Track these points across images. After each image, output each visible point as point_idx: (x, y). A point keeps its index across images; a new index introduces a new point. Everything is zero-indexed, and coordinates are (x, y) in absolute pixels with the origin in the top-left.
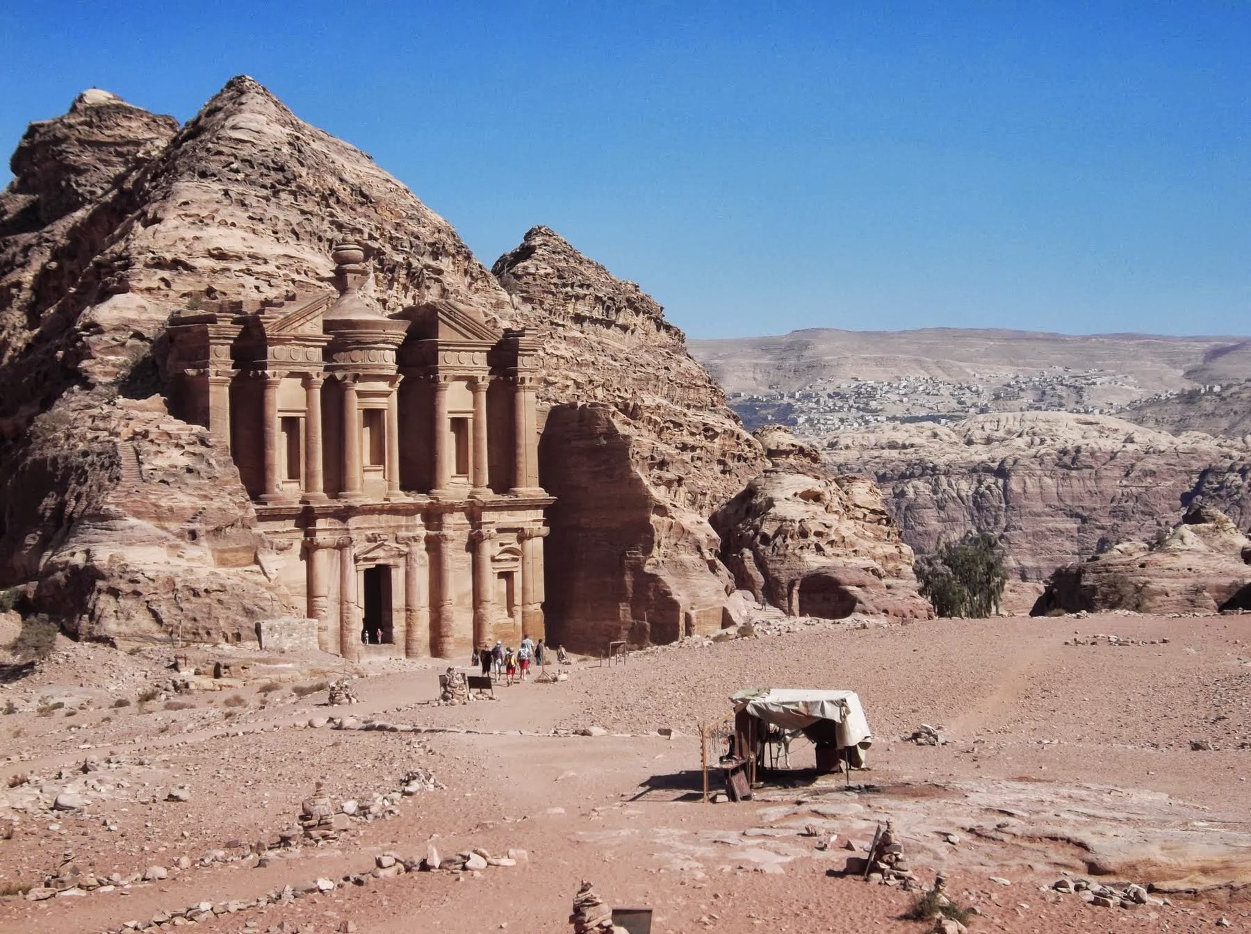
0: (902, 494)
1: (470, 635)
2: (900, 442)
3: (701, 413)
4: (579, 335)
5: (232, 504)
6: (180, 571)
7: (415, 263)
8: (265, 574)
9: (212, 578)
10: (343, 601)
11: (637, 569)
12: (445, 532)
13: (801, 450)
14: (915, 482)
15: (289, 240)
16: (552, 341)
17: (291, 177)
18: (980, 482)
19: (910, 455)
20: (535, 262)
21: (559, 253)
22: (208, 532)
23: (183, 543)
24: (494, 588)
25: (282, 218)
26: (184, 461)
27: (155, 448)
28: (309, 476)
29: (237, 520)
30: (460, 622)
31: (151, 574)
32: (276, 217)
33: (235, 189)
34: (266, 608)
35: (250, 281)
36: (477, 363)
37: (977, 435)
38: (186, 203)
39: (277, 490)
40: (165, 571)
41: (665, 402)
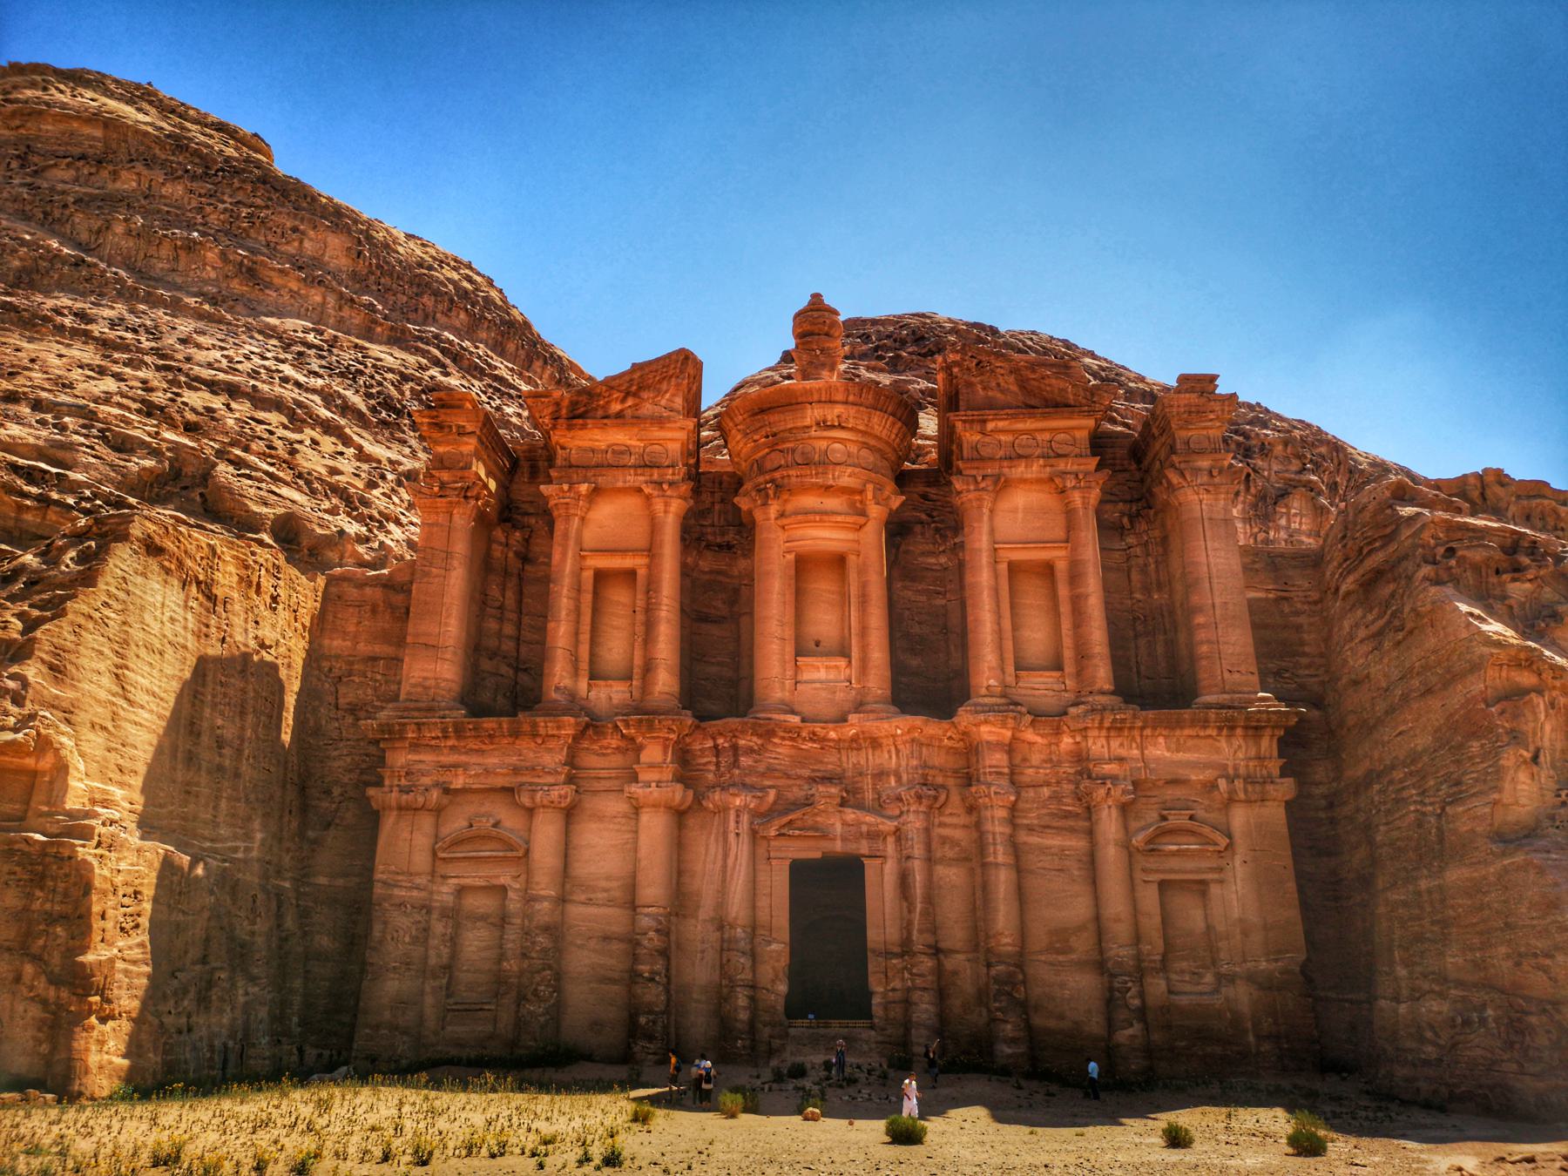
10: (721, 924)
28: (648, 668)
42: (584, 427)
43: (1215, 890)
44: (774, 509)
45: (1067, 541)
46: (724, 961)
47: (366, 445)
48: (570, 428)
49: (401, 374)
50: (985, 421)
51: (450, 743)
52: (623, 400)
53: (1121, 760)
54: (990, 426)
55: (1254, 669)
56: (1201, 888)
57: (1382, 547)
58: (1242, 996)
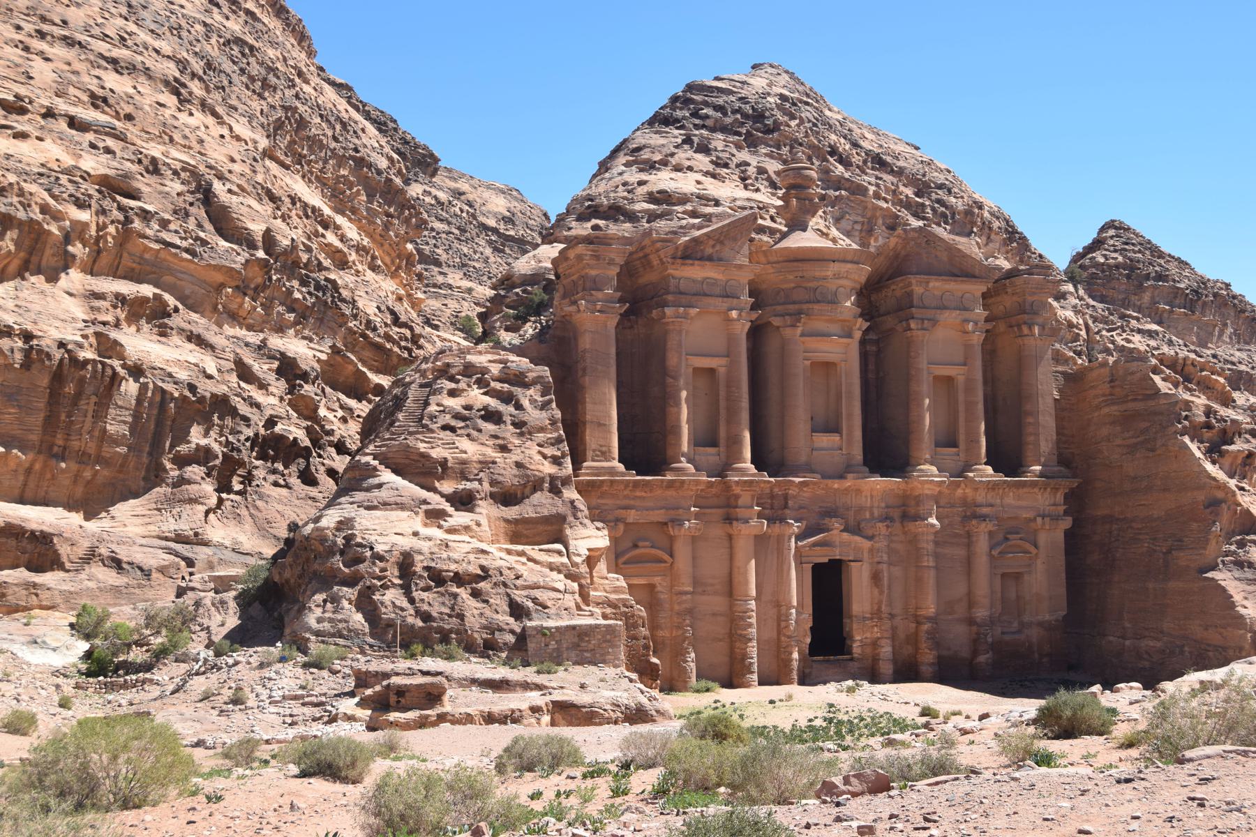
4: (1154, 327)
5: (539, 457)
6: (425, 546)
8: (568, 557)
9: (472, 557)
15: (762, 187)
16: (1124, 335)
17: (769, 122)
20: (1104, 252)
21: (1133, 244)
23: (450, 510)
25: (754, 163)
26: (487, 400)
27: (453, 385)
29: (542, 480)
31: (379, 548)
32: (748, 164)
34: (549, 604)
38: (638, 149)
39: (682, 459)
40: (406, 543)
42: (692, 265)
43: (1026, 577)
44: (799, 331)
45: (965, 364)
46: (783, 624)
47: (233, 125)
48: (683, 264)
49: (205, 25)
50: (928, 282)
51: (625, 493)
52: (713, 246)
53: (992, 505)
54: (931, 285)
55: (1055, 452)
56: (1018, 577)
57: (1141, 400)
58: (1034, 634)
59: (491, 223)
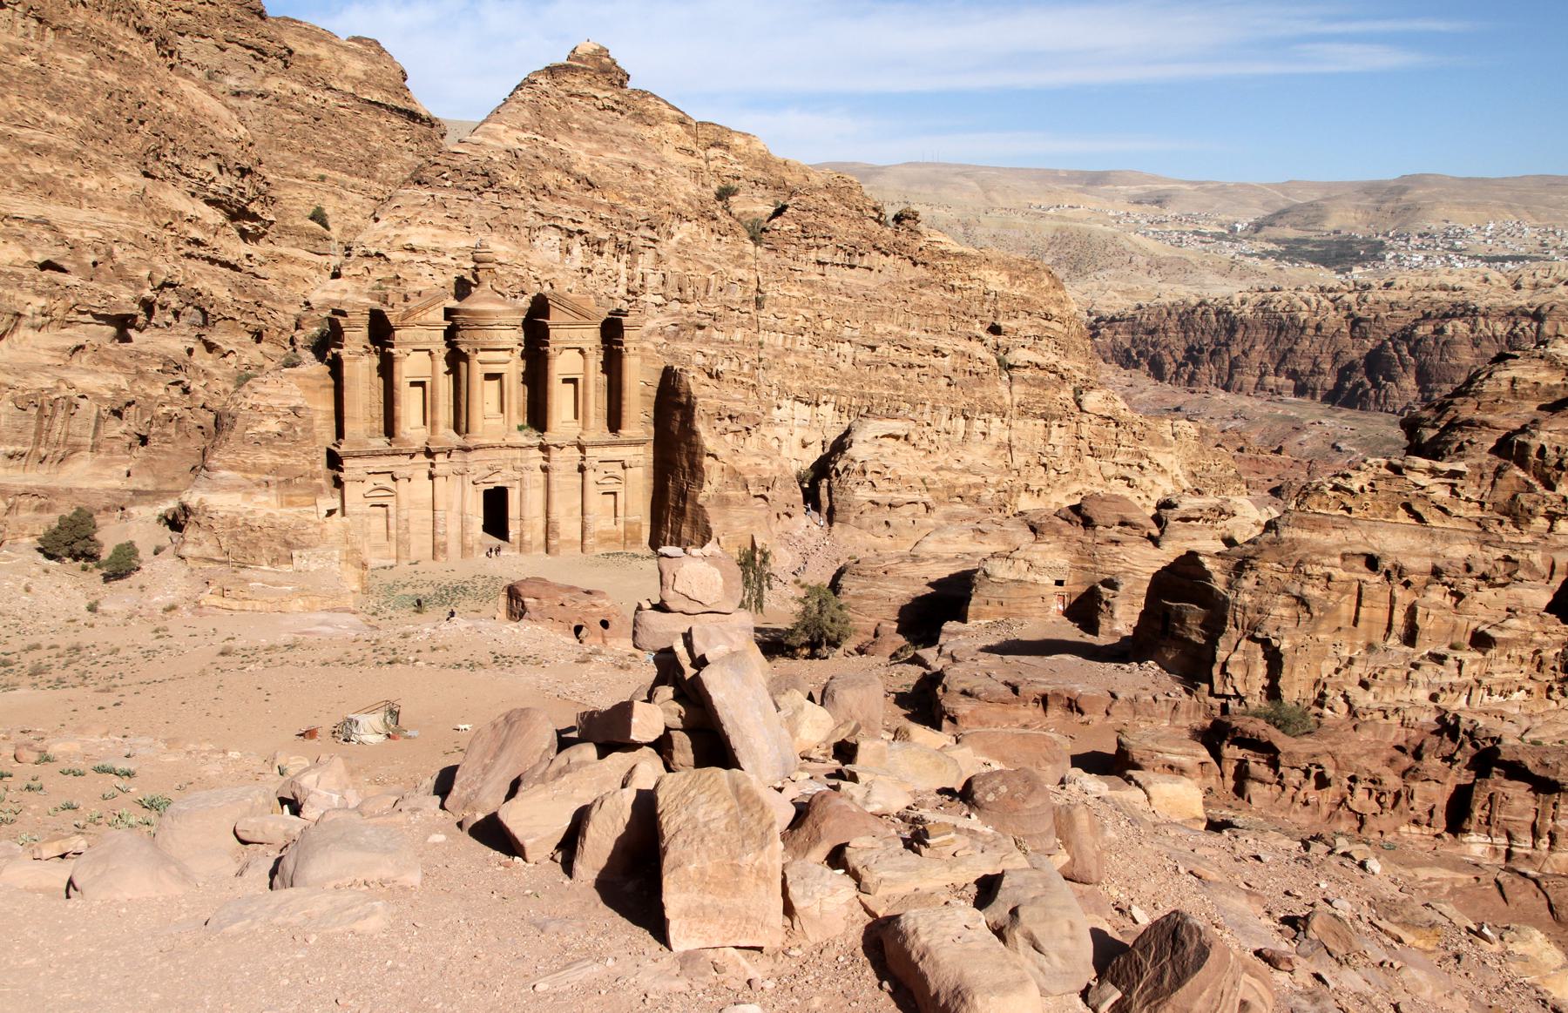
0: (1439, 331)
1: (579, 538)
2: (1450, 285)
3: (936, 336)
7: (623, 238)
11: (694, 499)
12: (552, 463)
13: (1037, 365)
14: (1455, 322)
16: (788, 284)
18: (1515, 324)
19: (1458, 297)
22: (279, 482)
24: (596, 502)
25: (476, 215)
28: (434, 424)
30: (569, 527)
31: (221, 514)
33: (439, 194)
35: (427, 269)
36: (591, 337)
37: (1526, 281)
41: (897, 329)
59: (349, 88)
